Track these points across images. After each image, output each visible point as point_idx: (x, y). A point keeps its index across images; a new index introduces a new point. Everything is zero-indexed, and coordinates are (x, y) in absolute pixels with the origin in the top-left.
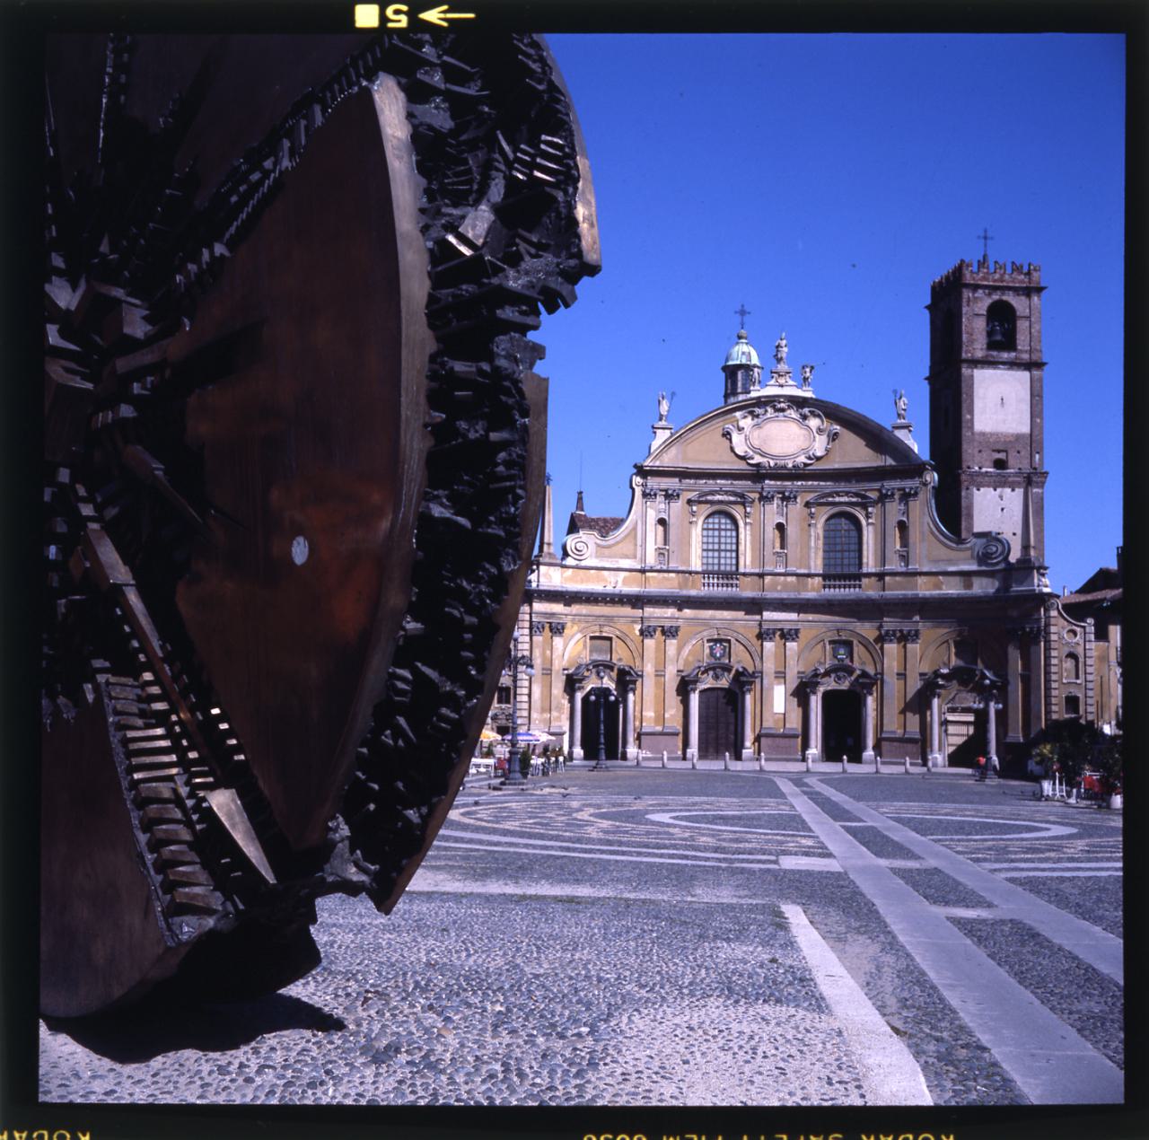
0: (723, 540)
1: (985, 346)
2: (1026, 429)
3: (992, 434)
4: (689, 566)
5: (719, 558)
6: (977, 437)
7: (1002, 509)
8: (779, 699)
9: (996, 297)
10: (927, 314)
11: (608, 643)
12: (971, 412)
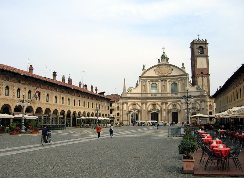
2: (206, 67)
8: (164, 114)
9: (200, 45)
11: (135, 106)
12: (197, 65)
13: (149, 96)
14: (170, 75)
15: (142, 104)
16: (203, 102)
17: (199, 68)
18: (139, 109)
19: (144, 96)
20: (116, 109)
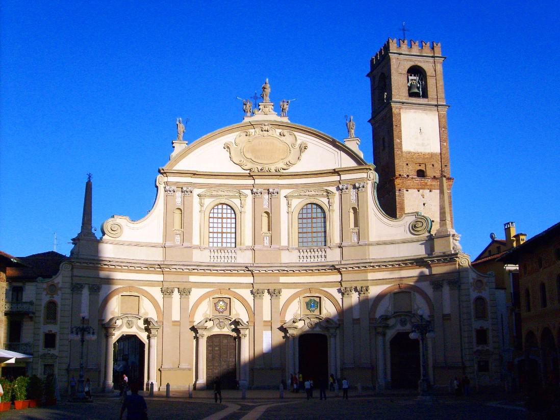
0: (225, 225)
1: (407, 94)
3: (415, 153)
4: (192, 242)
5: (222, 238)
6: (404, 155)
7: (424, 204)
10: (368, 80)
12: (400, 138)
13: (199, 257)
14: (292, 170)
15: (167, 292)
16: (446, 289)
17: (409, 153)
18: (149, 316)
19: (175, 257)
20: (42, 313)
